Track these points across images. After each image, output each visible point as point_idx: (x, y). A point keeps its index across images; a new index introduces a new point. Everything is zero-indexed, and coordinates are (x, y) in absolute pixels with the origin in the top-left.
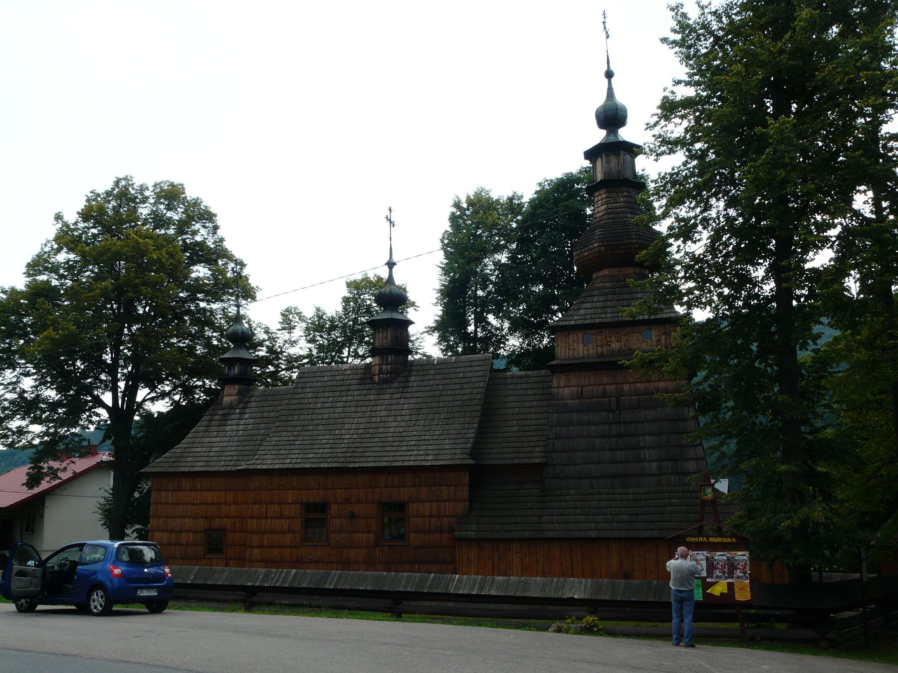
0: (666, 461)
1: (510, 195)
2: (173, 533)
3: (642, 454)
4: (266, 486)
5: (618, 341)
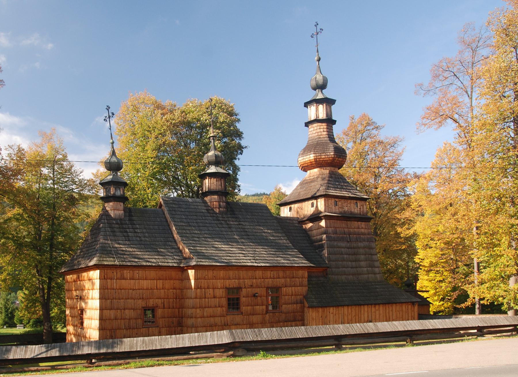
2: (119, 311)
4: (205, 277)
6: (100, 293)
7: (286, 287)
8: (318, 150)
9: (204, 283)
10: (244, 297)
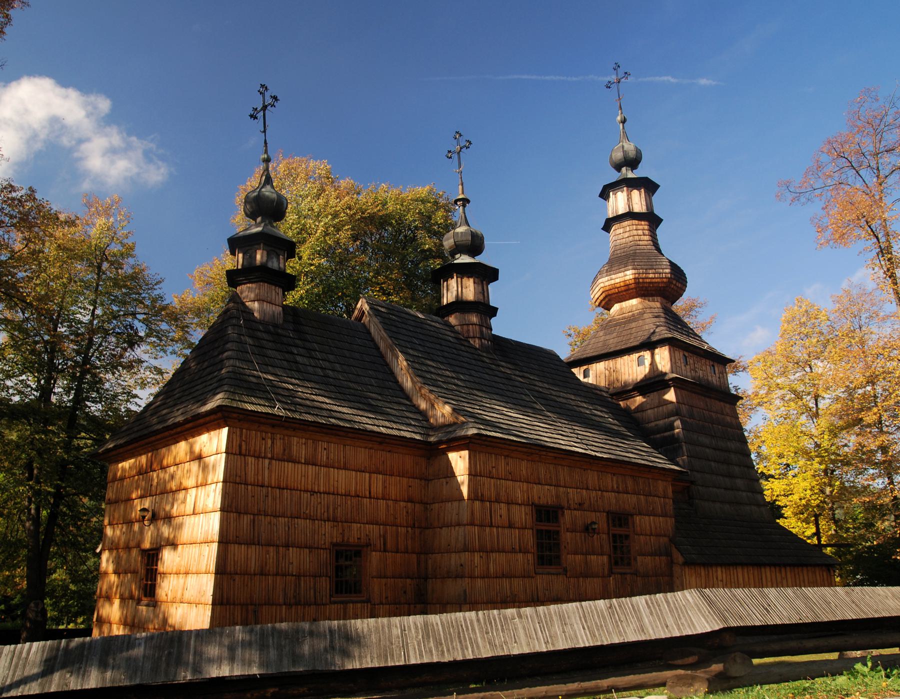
2: (271, 549)
4: (490, 472)
6: (225, 495)
7: (640, 514)
8: (640, 264)
9: (489, 486)
10: (568, 530)
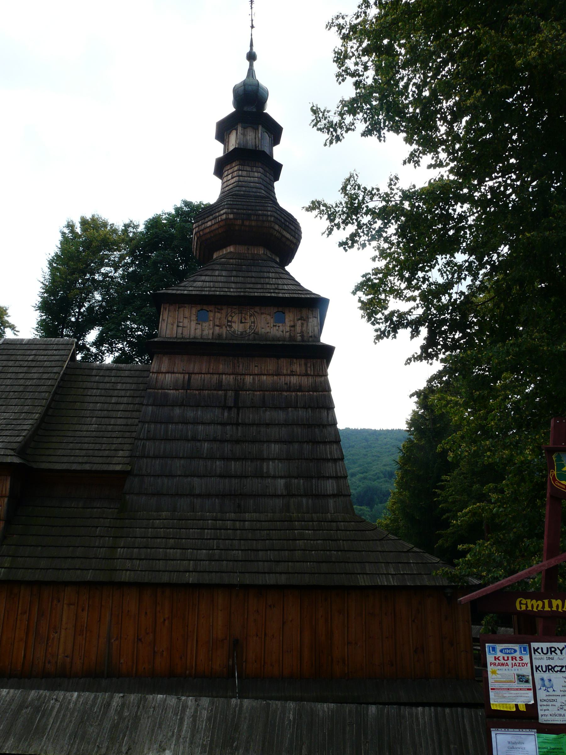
0: (296, 478)
1: (127, 222)
3: (265, 467)
5: (241, 322)
